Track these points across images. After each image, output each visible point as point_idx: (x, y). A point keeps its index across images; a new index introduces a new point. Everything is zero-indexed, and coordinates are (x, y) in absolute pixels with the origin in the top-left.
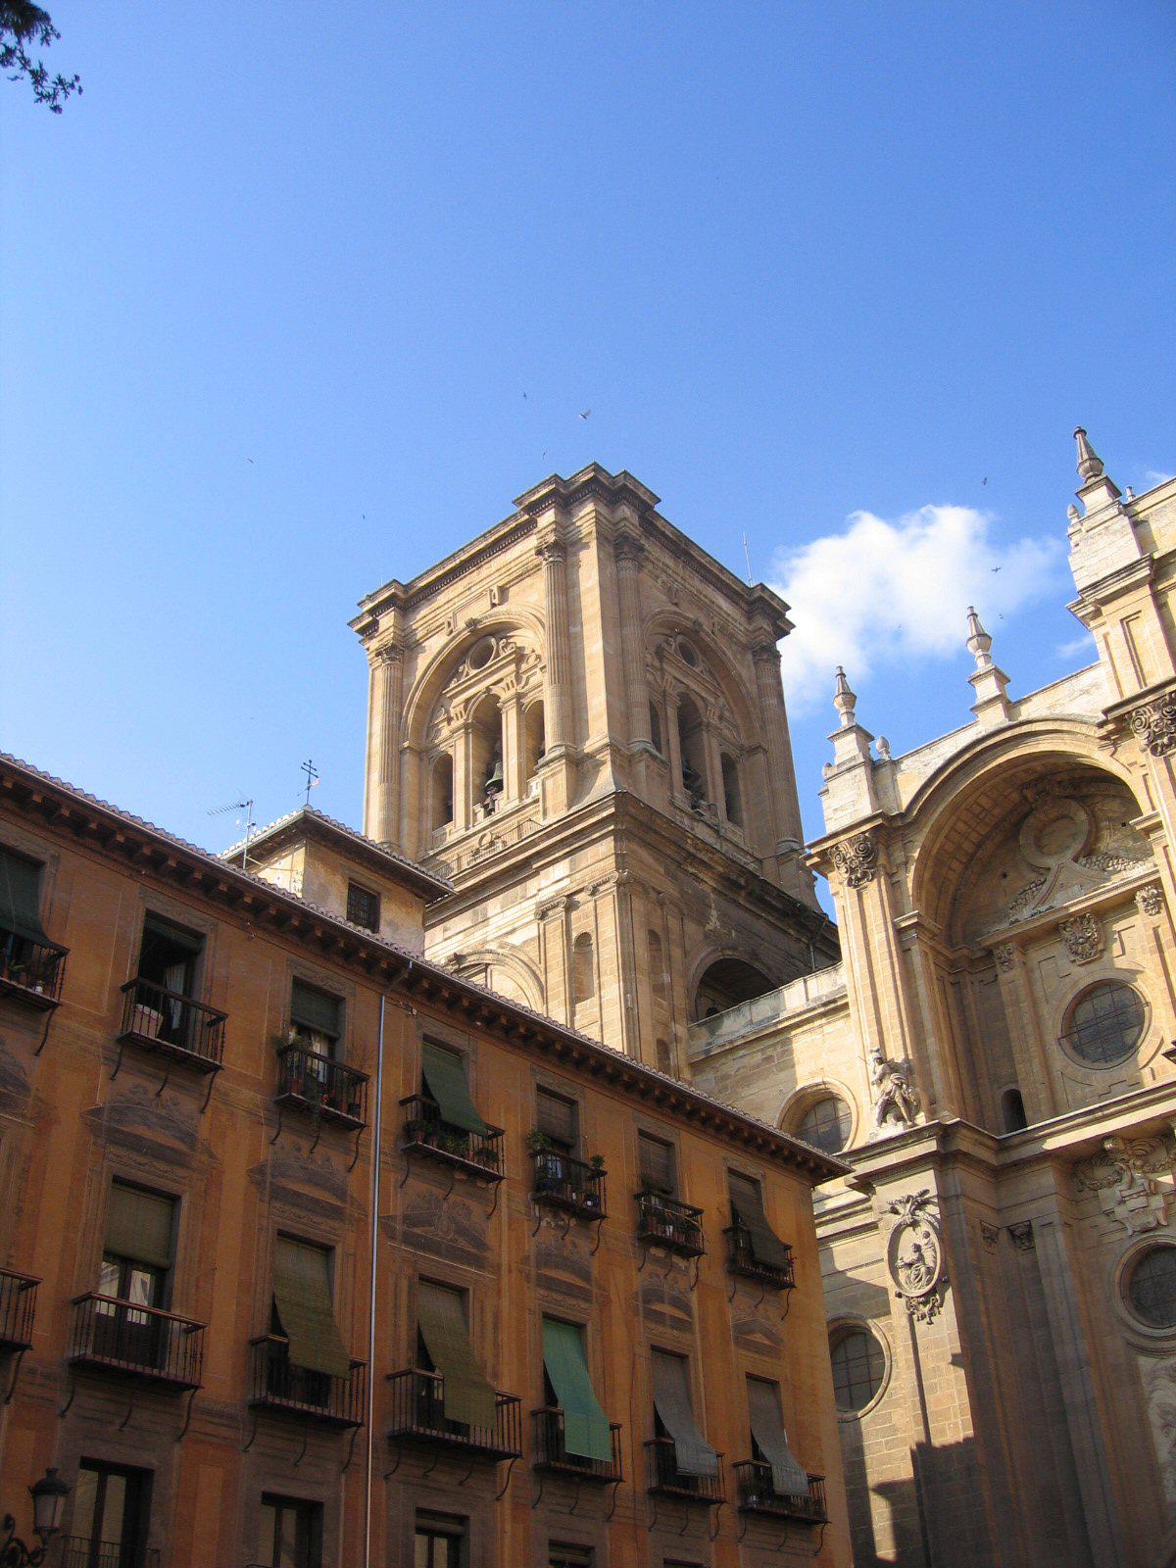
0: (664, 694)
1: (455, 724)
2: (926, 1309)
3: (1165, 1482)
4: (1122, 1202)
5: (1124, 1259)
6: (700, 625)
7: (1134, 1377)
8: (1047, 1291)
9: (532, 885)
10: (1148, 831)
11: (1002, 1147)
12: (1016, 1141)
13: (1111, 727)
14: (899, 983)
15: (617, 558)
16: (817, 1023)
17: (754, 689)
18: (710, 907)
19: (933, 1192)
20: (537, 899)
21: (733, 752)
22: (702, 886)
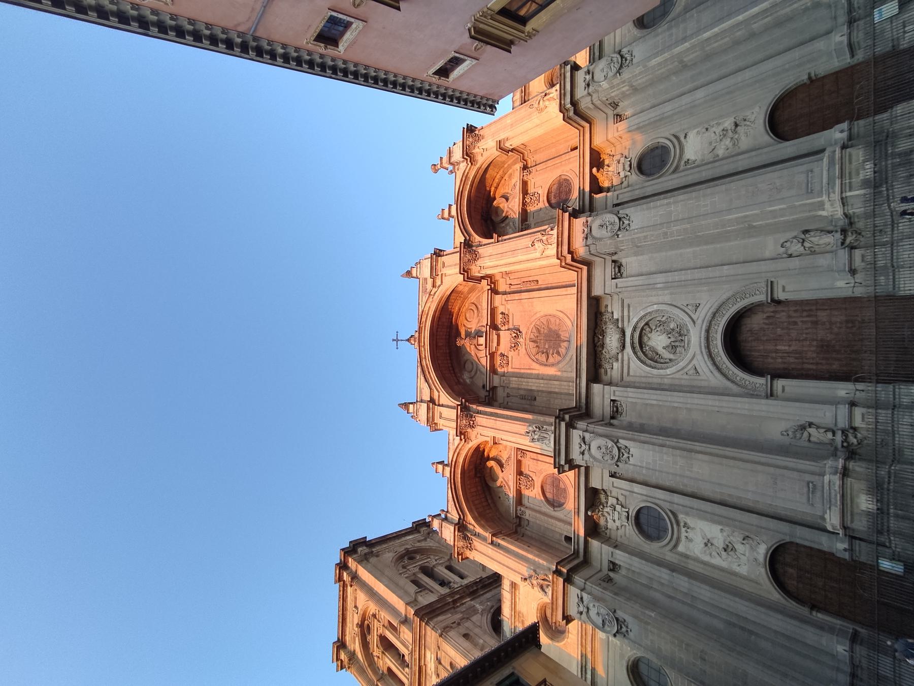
0: (414, 574)
1: (380, 657)
2: (624, 629)
3: (737, 571)
4: (614, 521)
5: (637, 532)
6: (407, 548)
7: (687, 557)
8: (637, 570)
9: (429, 671)
10: (495, 443)
11: (576, 553)
12: (576, 547)
13: (463, 437)
14: (506, 555)
15: (368, 561)
16: (517, 594)
17: (437, 545)
18: (474, 606)
19: (579, 592)
20: (433, 673)
21: (447, 564)
22: (467, 604)
